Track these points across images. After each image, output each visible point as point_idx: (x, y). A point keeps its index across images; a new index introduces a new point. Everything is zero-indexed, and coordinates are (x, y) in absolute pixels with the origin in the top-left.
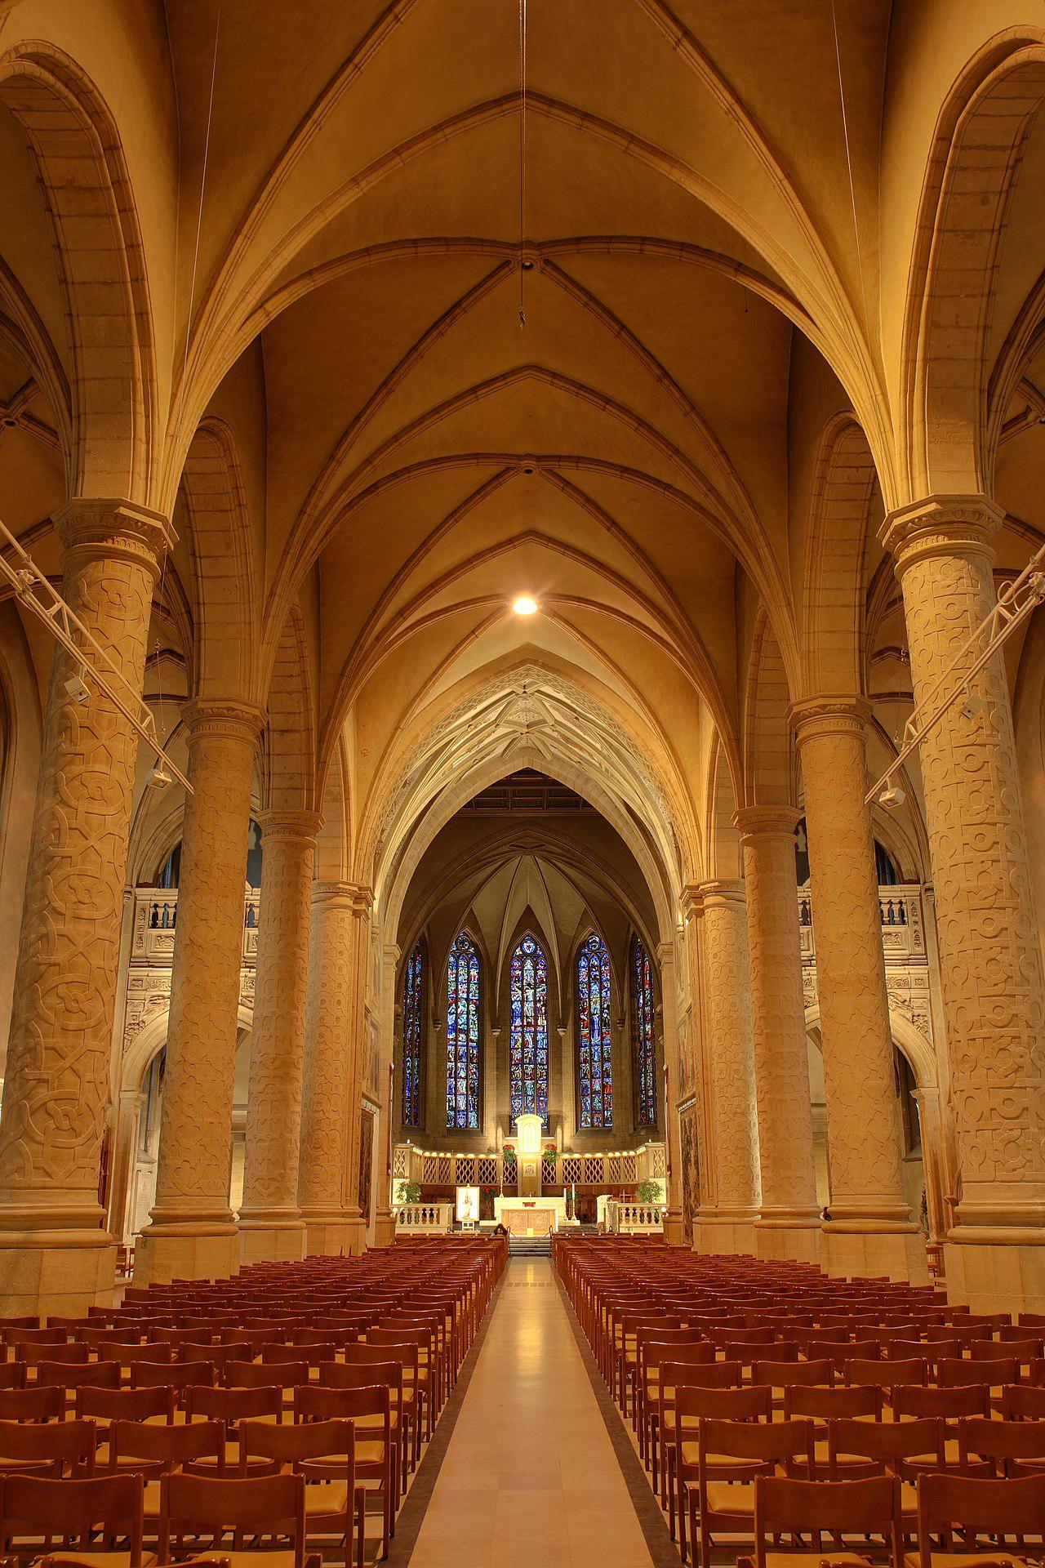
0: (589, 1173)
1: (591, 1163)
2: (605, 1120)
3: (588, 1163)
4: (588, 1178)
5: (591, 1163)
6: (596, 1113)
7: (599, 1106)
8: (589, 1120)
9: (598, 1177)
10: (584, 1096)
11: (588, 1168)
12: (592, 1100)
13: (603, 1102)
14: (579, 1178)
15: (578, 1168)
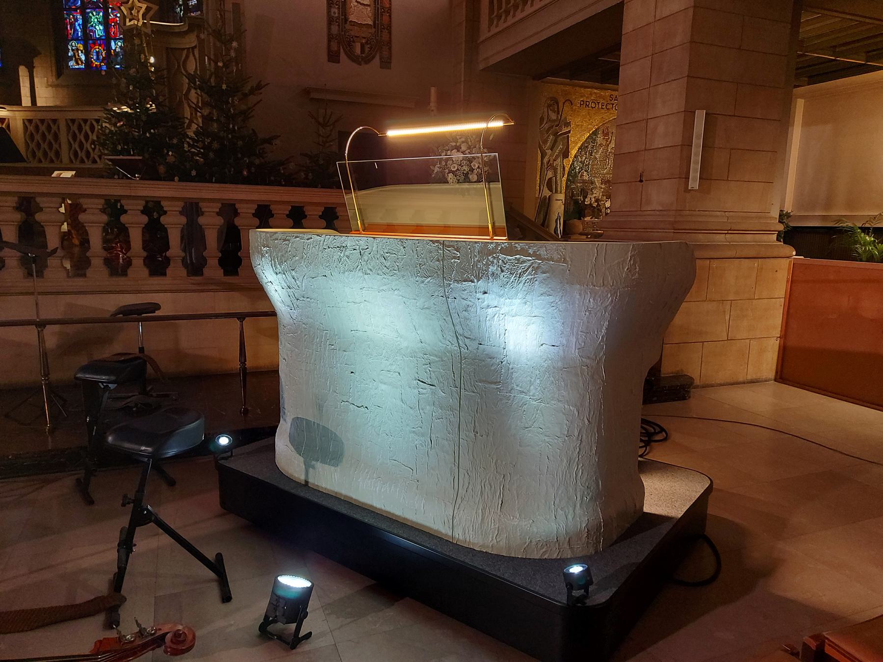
0: (76, 146)
1: (80, 128)
2: (110, 58)
3: (75, 128)
4: (76, 154)
5: (80, 128)
6: (95, 44)
7: (99, 30)
8: (83, 58)
9: (52, 154)
10: (70, 10)
11: (75, 137)
12: (86, 20)
13: (106, 23)
14: (58, 154)
15: (56, 137)
